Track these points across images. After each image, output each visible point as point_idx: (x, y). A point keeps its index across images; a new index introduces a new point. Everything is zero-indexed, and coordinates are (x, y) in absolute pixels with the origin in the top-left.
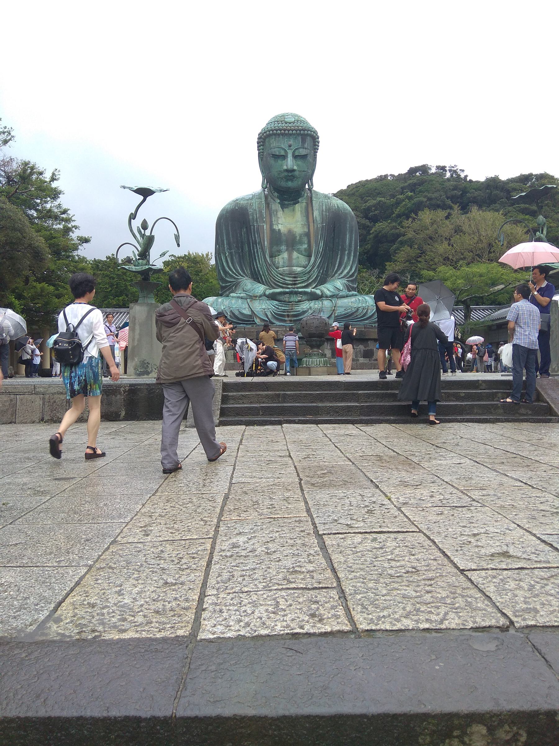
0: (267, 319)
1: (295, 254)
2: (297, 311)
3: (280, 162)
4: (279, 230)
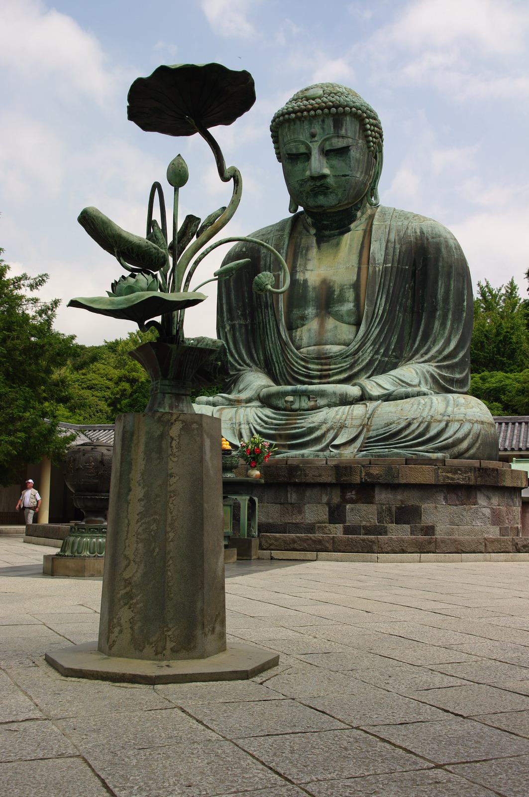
1: (331, 323)
2: (298, 428)
3: (300, 166)
4: (305, 281)
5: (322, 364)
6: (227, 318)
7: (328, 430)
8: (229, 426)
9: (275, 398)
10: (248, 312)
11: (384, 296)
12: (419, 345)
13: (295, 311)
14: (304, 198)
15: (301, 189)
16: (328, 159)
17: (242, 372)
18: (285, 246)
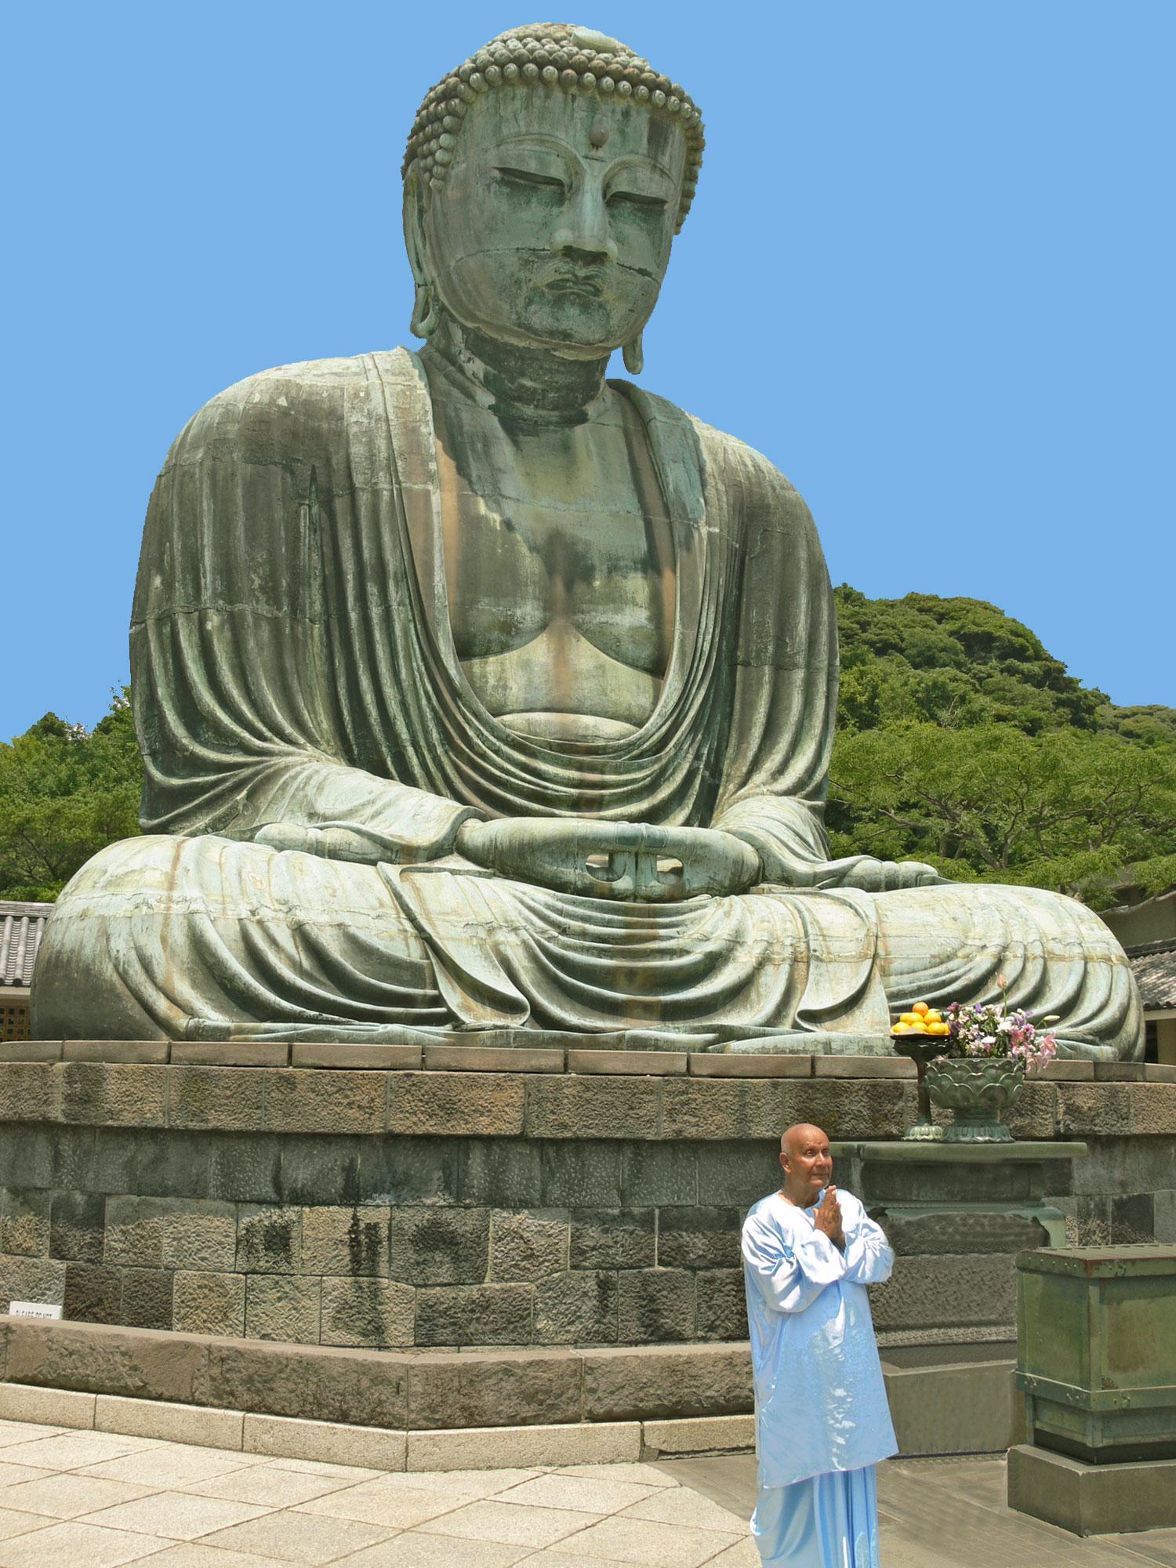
0: (512, 991)
1: (585, 655)
3: (534, 211)
5: (580, 767)
6: (214, 589)
7: (760, 965)
8: (460, 932)
9: (551, 854)
10: (284, 584)
11: (713, 608)
12: (760, 749)
13: (484, 603)
14: (521, 302)
15: (522, 275)
16: (612, 216)
17: (282, 761)
18: (430, 417)
